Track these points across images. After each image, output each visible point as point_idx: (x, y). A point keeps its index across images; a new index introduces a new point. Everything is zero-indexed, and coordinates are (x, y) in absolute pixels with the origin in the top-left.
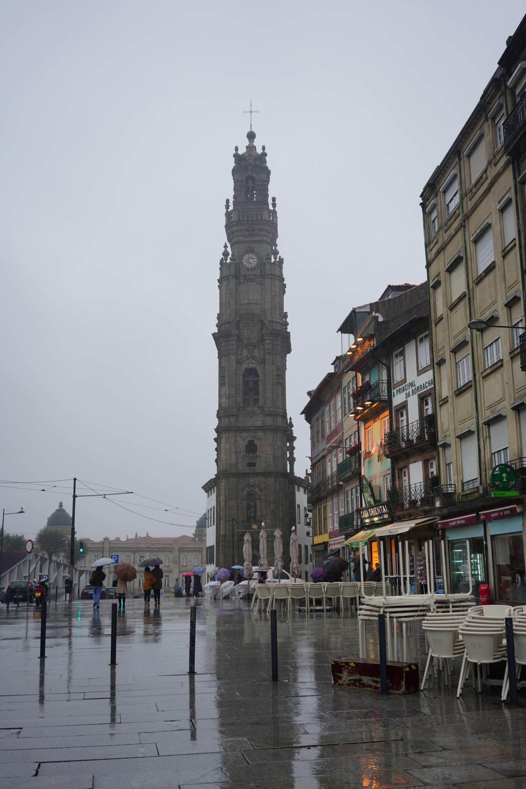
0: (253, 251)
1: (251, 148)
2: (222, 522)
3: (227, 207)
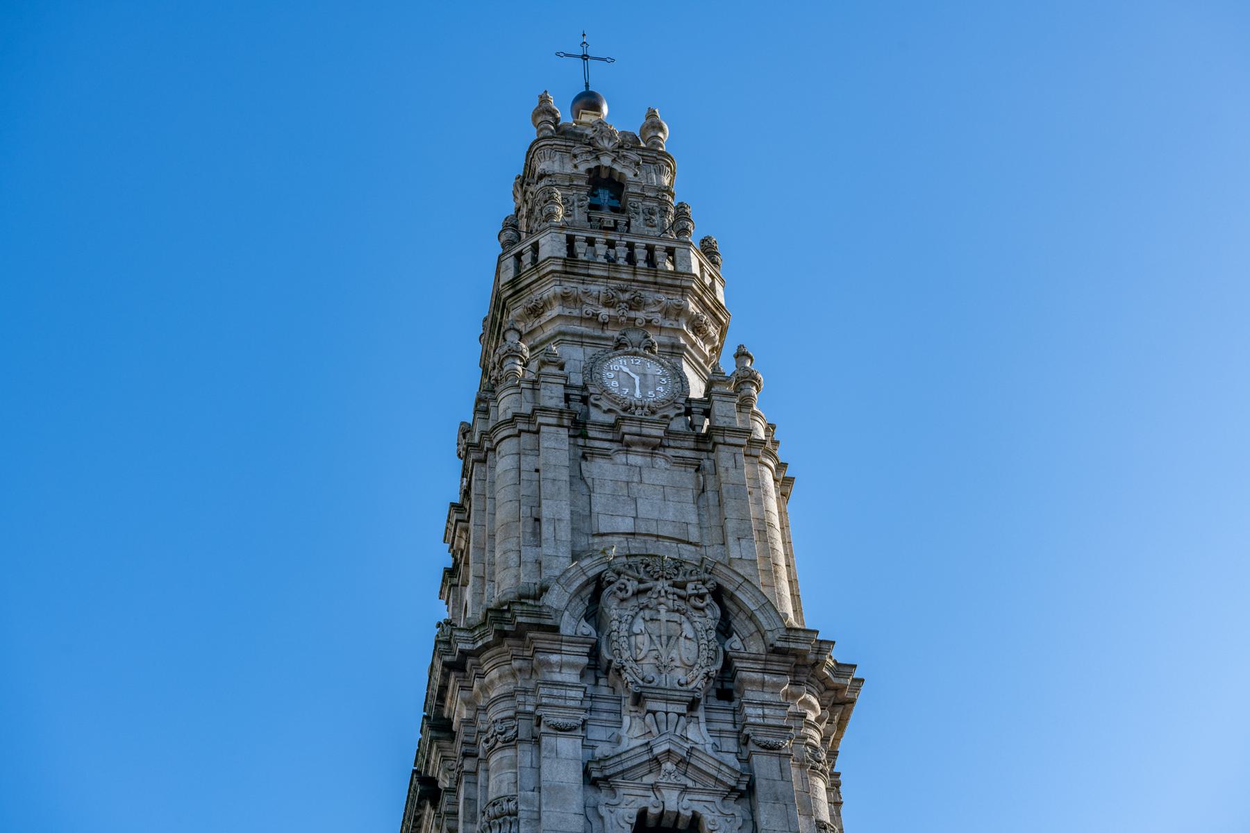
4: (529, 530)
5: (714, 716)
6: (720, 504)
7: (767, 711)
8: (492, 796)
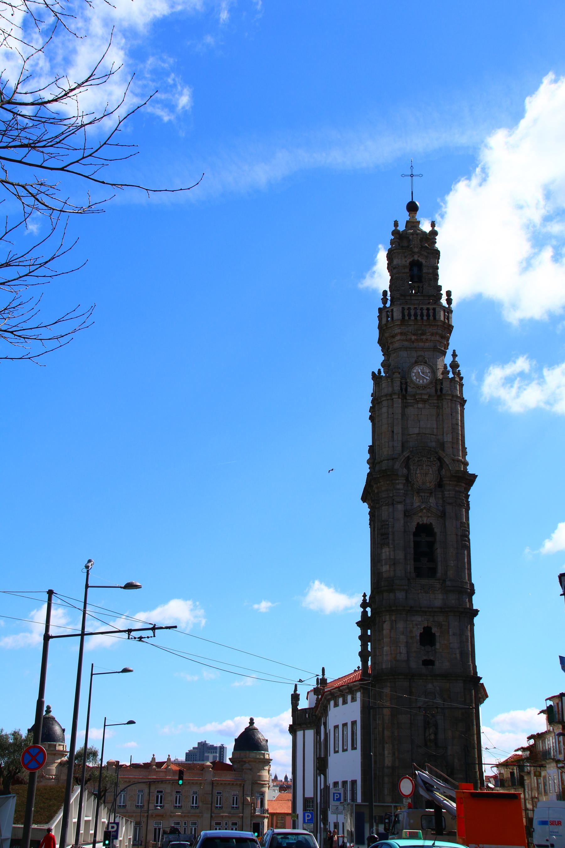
0: (426, 363)
1: (413, 224)
2: (386, 746)
3: (384, 300)
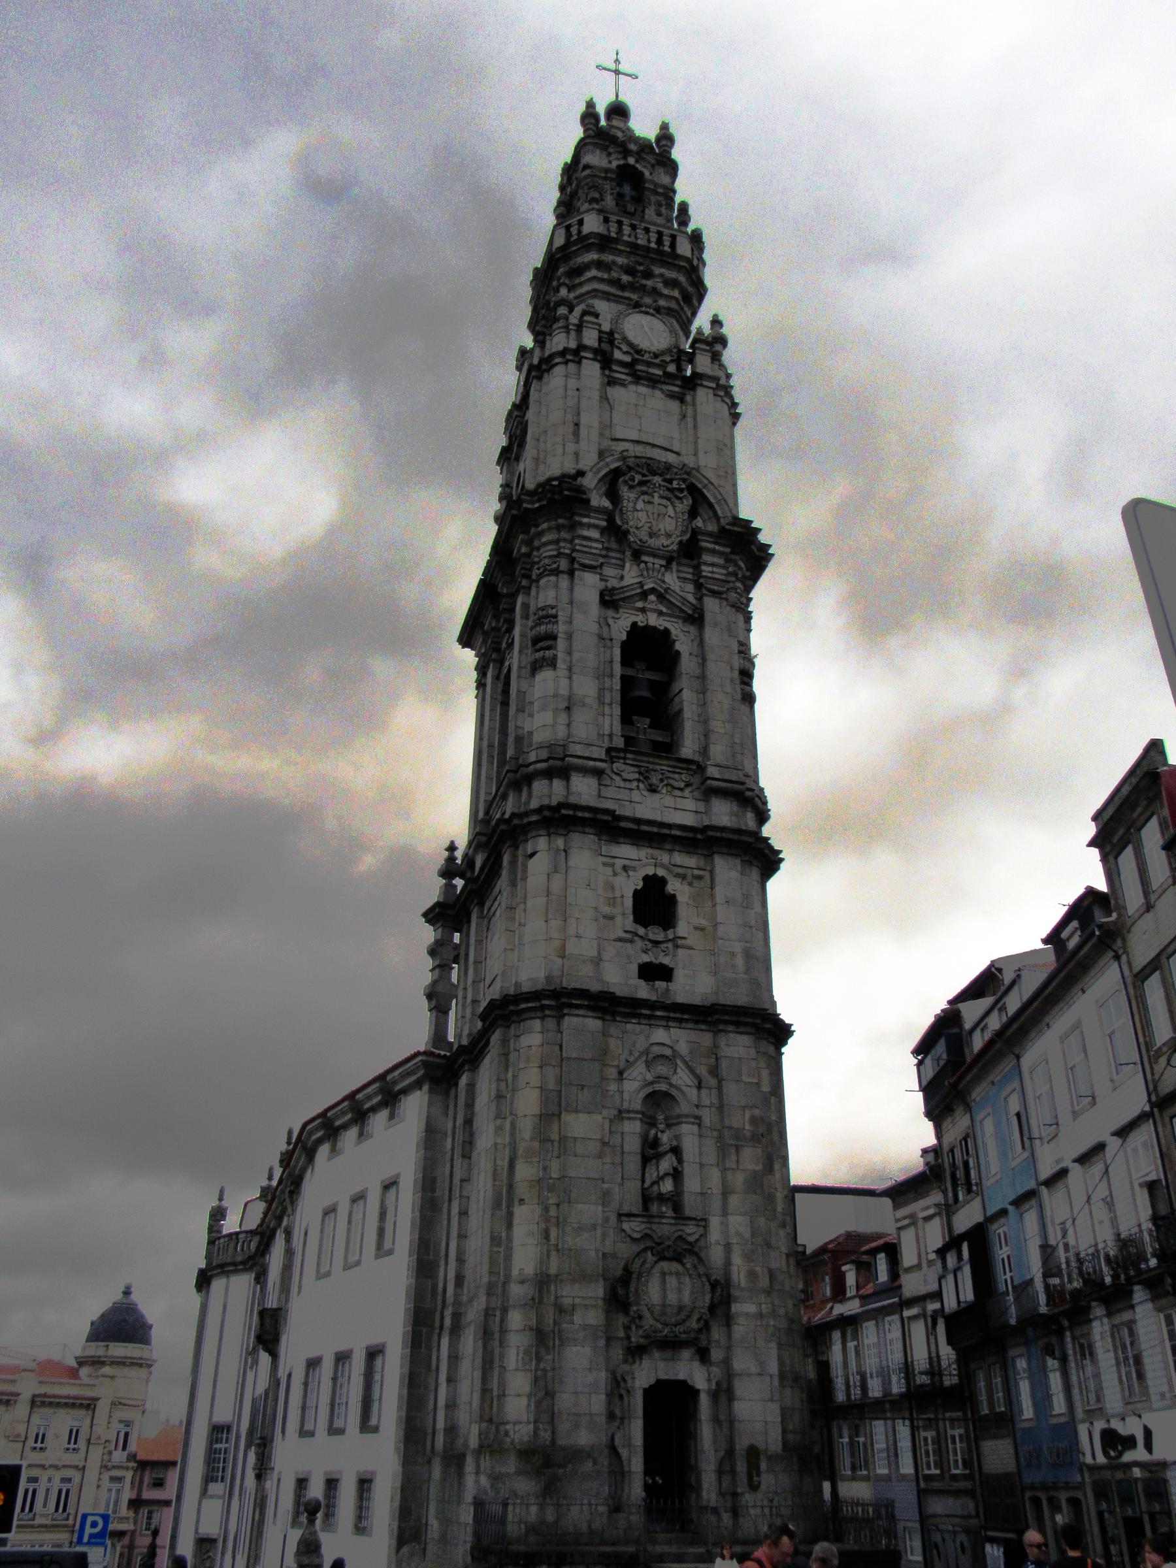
2: (520, 1212)
4: (571, 430)
5: (682, 568)
6: (695, 427)
7: (715, 569)
8: (541, 605)
